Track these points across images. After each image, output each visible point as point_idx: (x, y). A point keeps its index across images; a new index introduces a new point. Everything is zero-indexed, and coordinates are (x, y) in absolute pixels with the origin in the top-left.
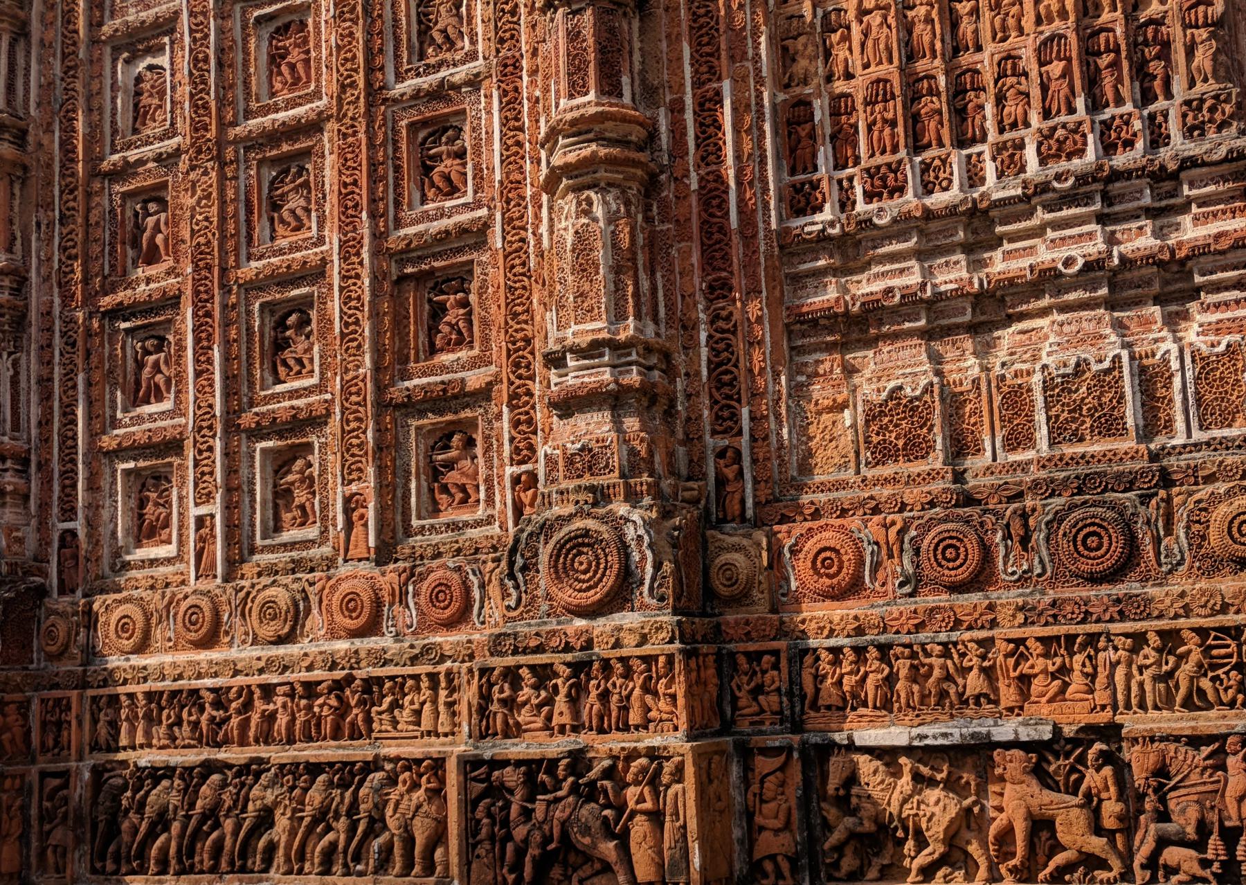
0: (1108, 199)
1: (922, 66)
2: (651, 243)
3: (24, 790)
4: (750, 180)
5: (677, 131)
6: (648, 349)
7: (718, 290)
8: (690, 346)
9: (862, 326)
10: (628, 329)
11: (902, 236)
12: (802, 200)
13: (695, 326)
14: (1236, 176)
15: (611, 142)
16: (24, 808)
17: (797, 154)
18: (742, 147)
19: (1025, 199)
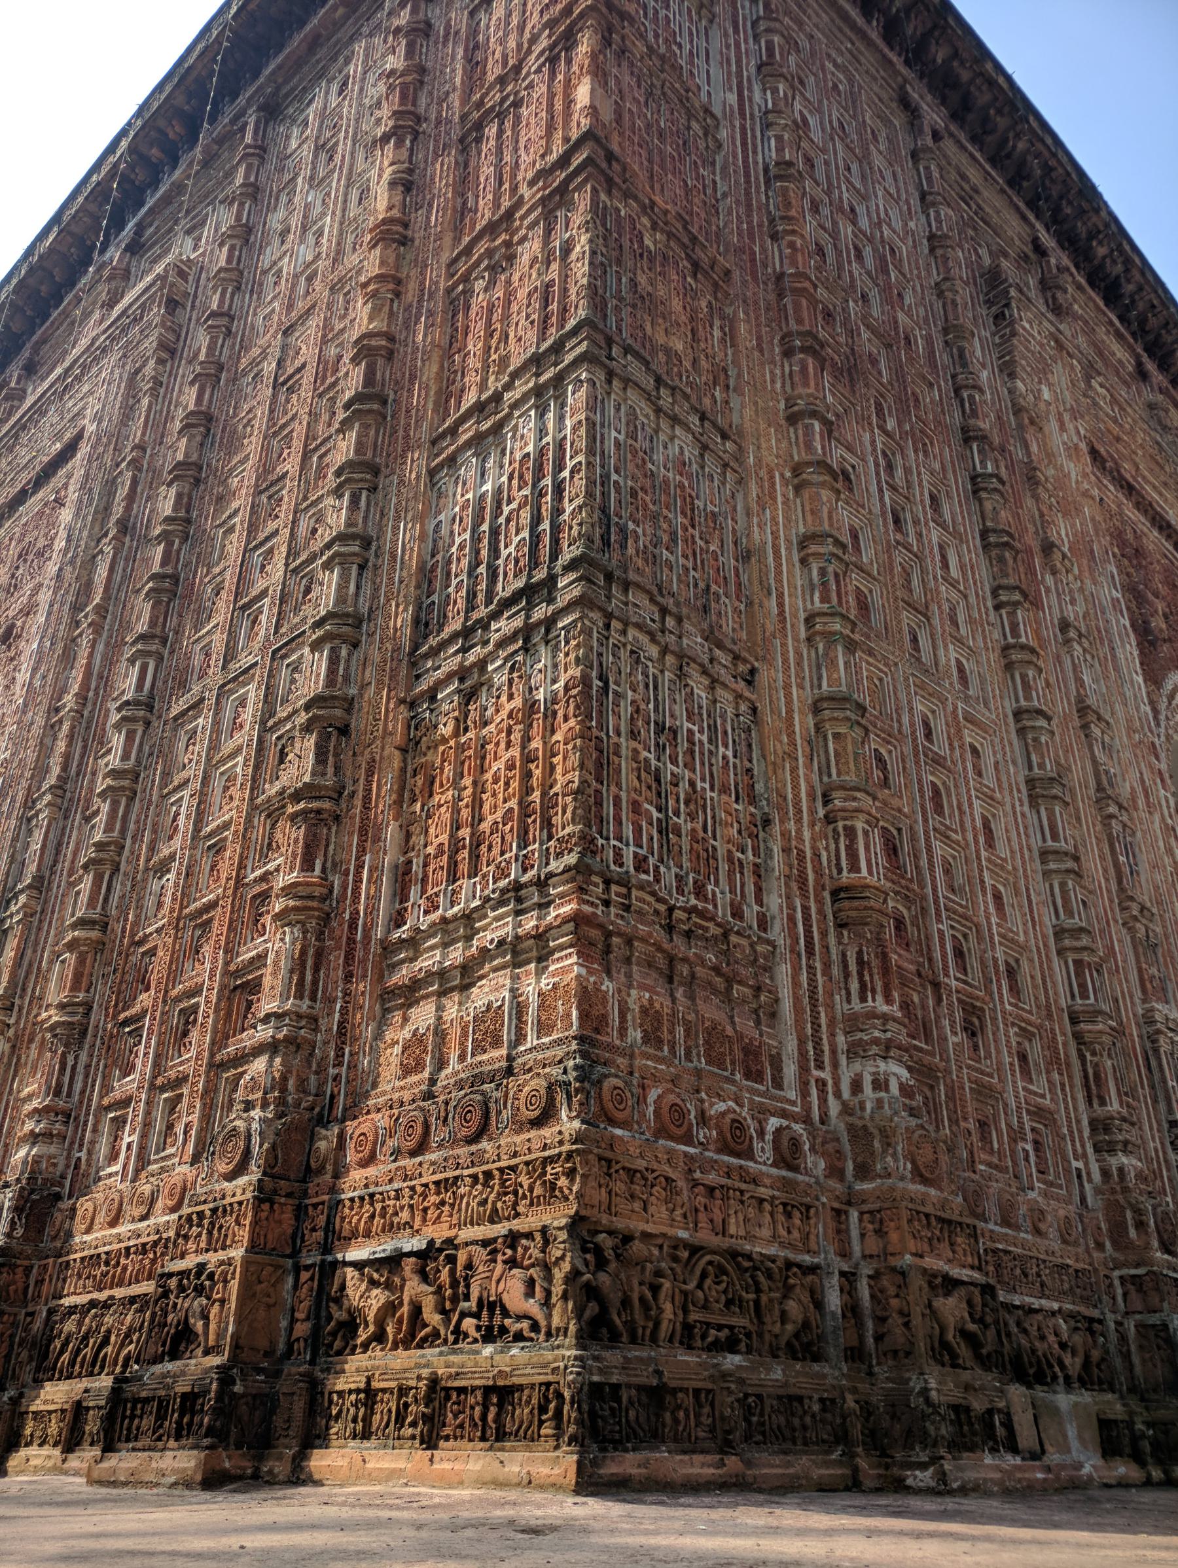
0: (519, 900)
1: (461, 833)
2: (320, 954)
3: (14, 1325)
4: (371, 911)
5: (344, 887)
6: (300, 1016)
7: (348, 977)
8: (330, 1014)
9: (411, 993)
10: (288, 1005)
11: (434, 935)
12: (398, 920)
13: (334, 1001)
14: (573, 880)
15: (301, 898)
16: (12, 1336)
17: (401, 894)
18: (372, 895)
19: (482, 907)
